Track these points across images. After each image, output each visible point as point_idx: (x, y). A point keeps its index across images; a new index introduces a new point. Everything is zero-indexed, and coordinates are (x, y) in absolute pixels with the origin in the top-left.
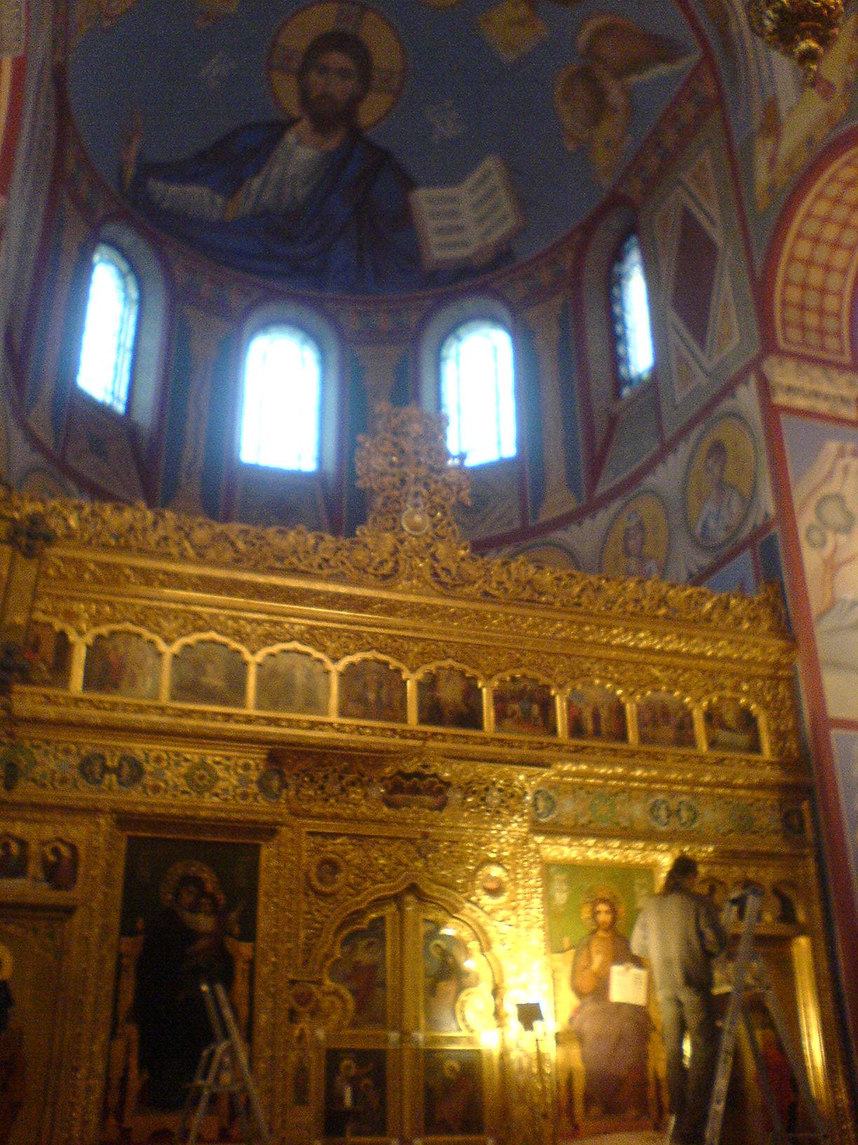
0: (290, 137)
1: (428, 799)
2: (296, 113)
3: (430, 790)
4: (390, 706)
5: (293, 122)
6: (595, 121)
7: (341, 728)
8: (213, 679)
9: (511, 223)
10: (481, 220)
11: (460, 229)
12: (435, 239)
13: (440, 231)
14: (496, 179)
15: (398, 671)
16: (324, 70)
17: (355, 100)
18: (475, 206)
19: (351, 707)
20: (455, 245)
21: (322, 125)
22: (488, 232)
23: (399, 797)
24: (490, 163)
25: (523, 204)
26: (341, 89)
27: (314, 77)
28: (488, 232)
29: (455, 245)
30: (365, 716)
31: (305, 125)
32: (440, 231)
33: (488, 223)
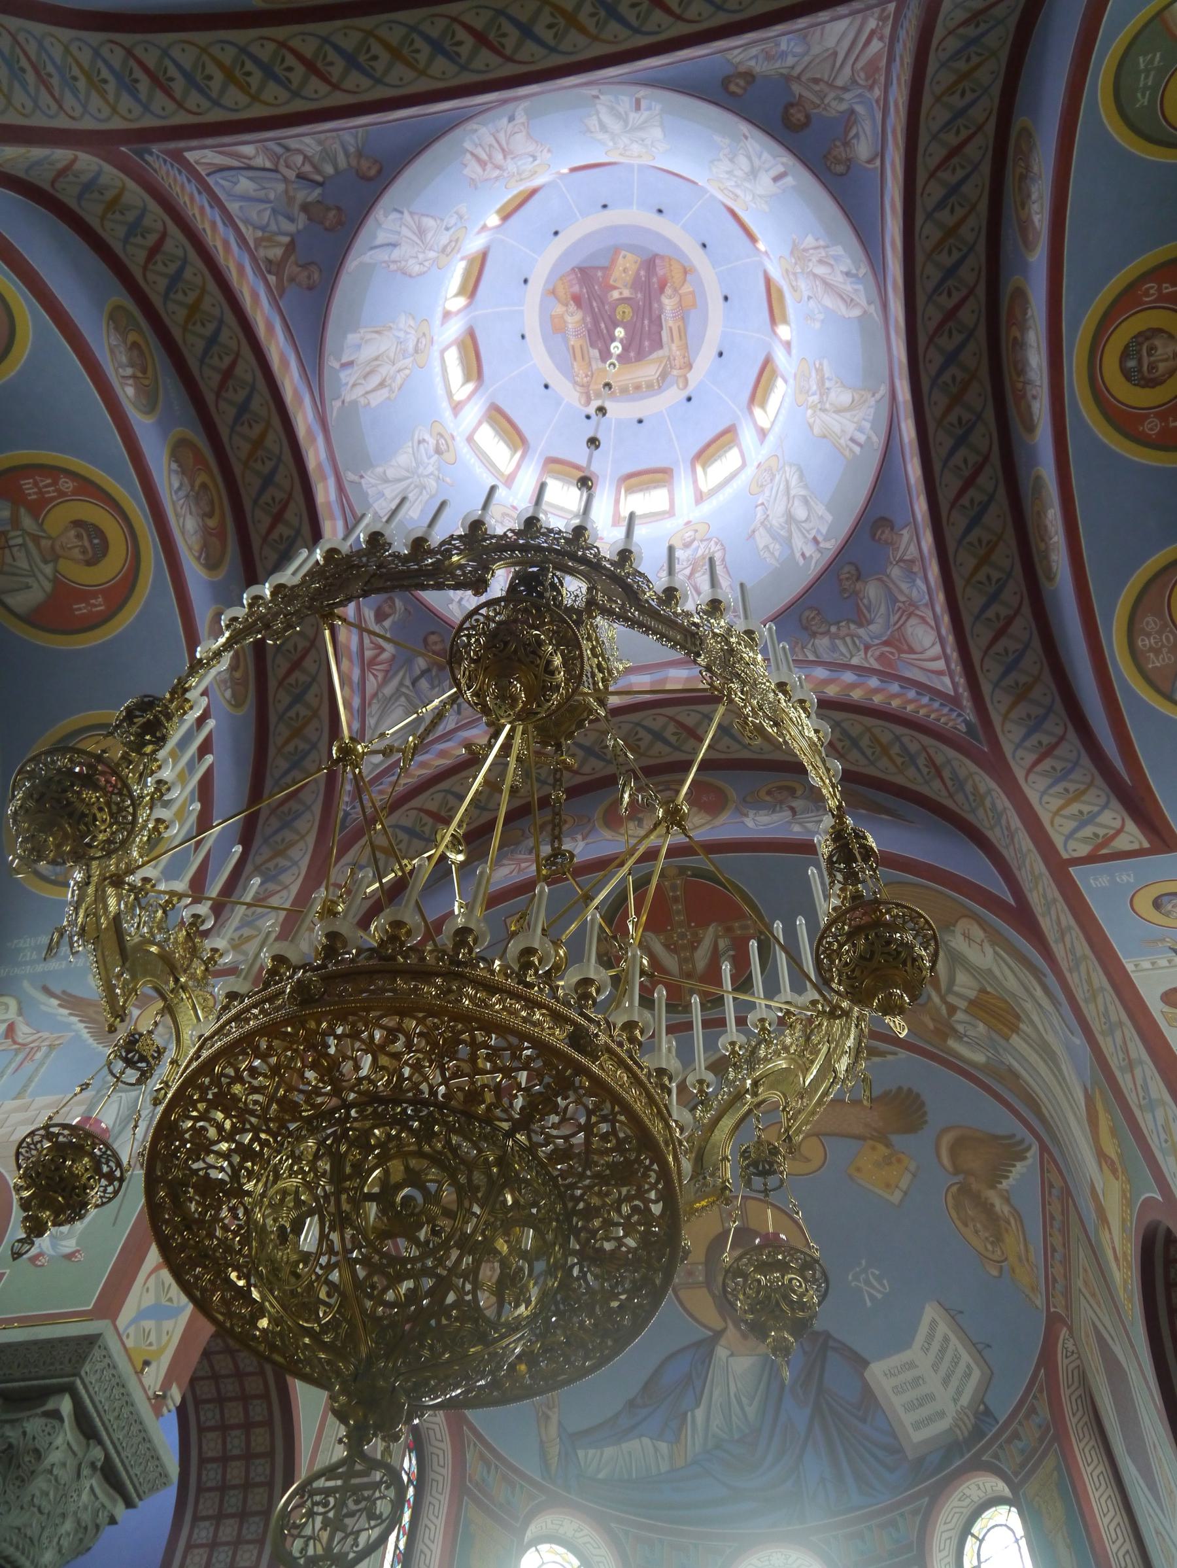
6: (998, 1239)
9: (976, 1374)
10: (946, 1382)
11: (930, 1397)
12: (908, 1419)
13: (910, 1407)
14: (943, 1328)
18: (935, 1367)
20: (930, 1420)
22: (959, 1392)
24: (930, 1312)
25: (979, 1349)
28: (959, 1392)
29: (930, 1420)
32: (910, 1407)
33: (954, 1383)
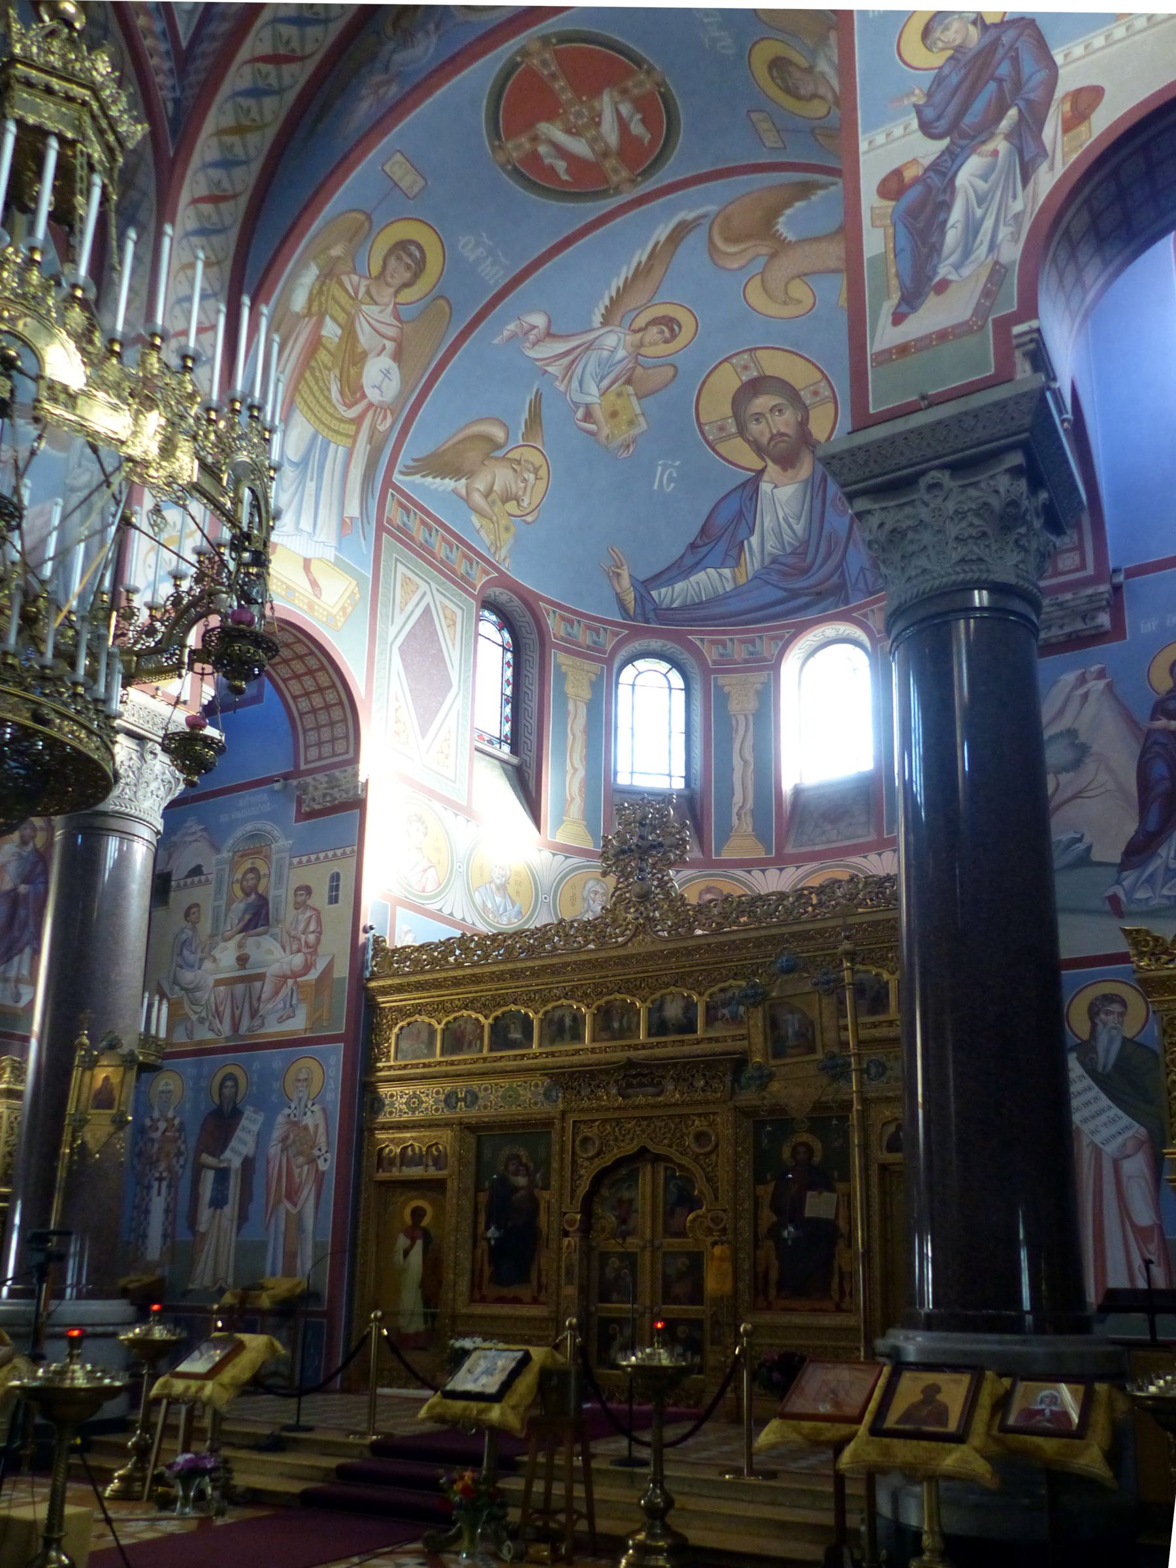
0: (765, 487)
1: (651, 1090)
2: (758, 464)
3: (652, 1084)
4: (629, 1028)
5: (761, 472)
7: (593, 1051)
8: (516, 1035)
15: (633, 1003)
16: (758, 417)
17: (803, 424)
19: (604, 1035)
21: (787, 461)
23: (630, 1091)
26: (785, 422)
27: (754, 428)
30: (614, 1039)
31: (772, 469)
